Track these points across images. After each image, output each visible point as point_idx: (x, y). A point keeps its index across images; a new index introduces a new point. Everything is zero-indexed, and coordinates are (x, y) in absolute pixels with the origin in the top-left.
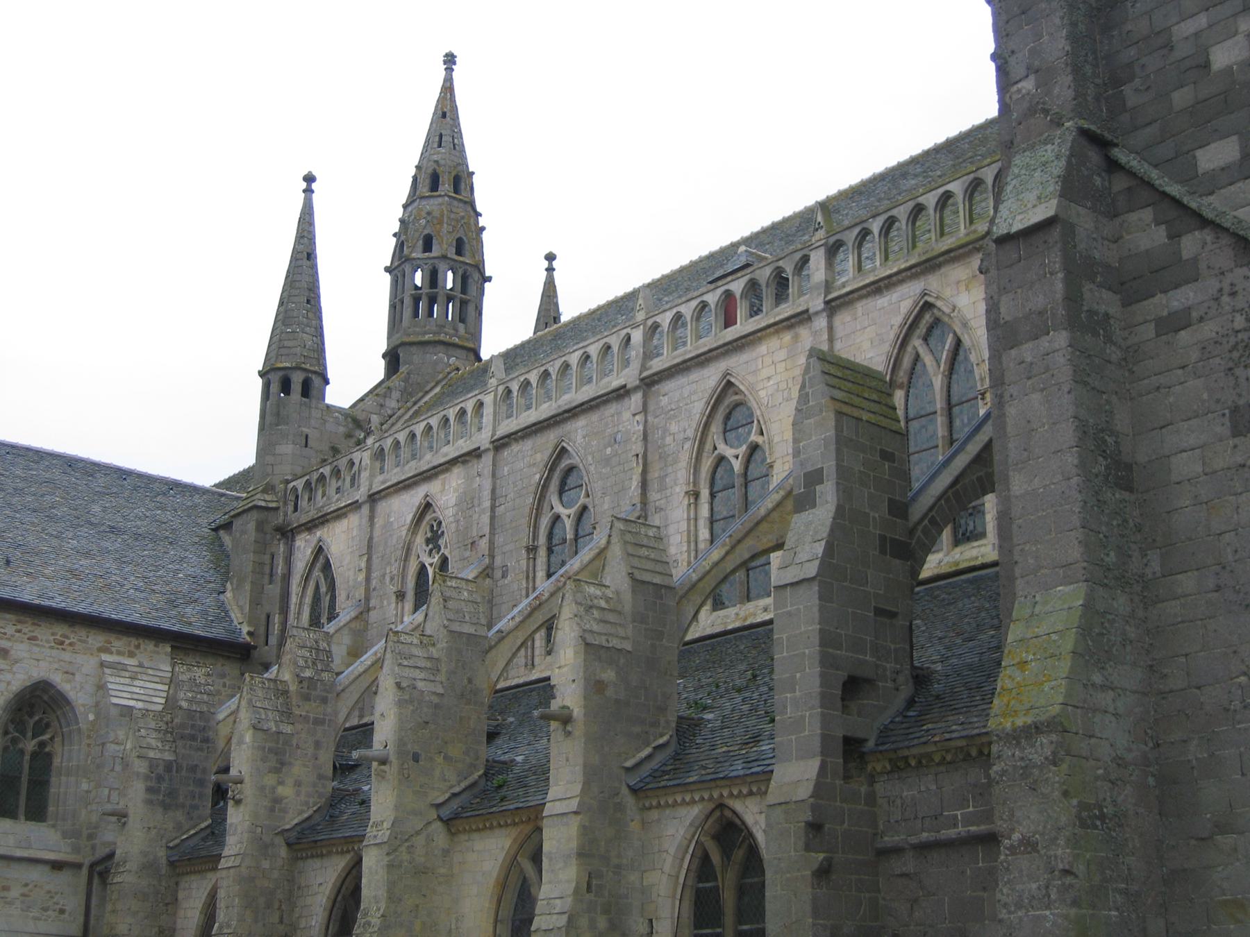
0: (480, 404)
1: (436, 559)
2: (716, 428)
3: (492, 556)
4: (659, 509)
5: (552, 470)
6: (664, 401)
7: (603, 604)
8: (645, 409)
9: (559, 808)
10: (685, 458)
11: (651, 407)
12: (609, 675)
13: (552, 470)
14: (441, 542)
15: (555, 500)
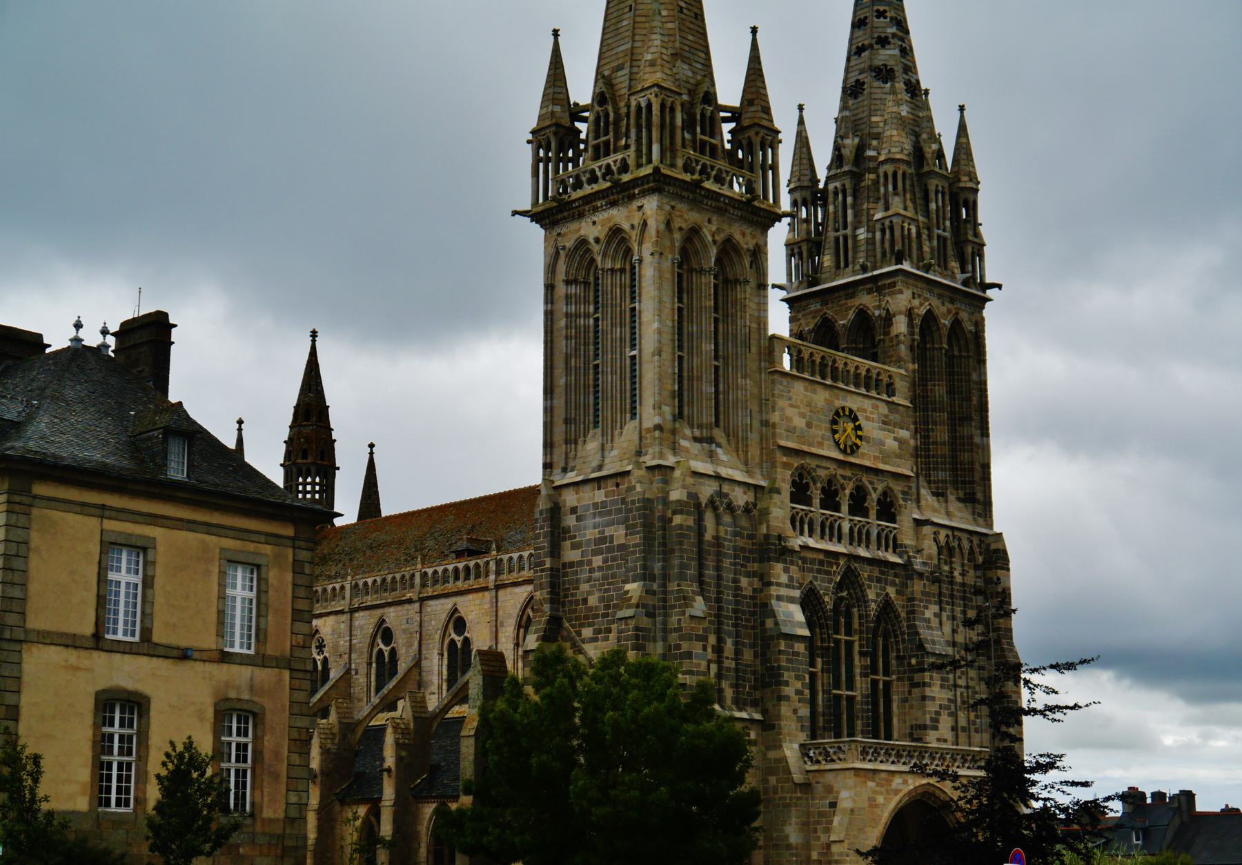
0: (342, 588)
1: (321, 657)
2: (451, 626)
3: (350, 664)
4: (426, 658)
5: (379, 628)
6: (429, 609)
7: (403, 726)
8: (421, 612)
9: (387, 803)
10: (437, 636)
11: (424, 611)
12: (404, 754)
13: (379, 628)
14: (325, 649)
15: (379, 641)
